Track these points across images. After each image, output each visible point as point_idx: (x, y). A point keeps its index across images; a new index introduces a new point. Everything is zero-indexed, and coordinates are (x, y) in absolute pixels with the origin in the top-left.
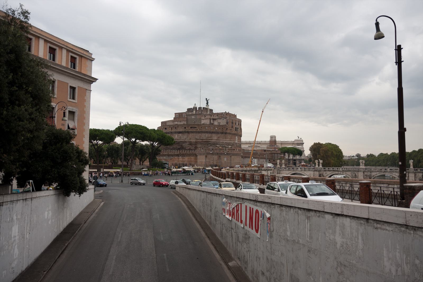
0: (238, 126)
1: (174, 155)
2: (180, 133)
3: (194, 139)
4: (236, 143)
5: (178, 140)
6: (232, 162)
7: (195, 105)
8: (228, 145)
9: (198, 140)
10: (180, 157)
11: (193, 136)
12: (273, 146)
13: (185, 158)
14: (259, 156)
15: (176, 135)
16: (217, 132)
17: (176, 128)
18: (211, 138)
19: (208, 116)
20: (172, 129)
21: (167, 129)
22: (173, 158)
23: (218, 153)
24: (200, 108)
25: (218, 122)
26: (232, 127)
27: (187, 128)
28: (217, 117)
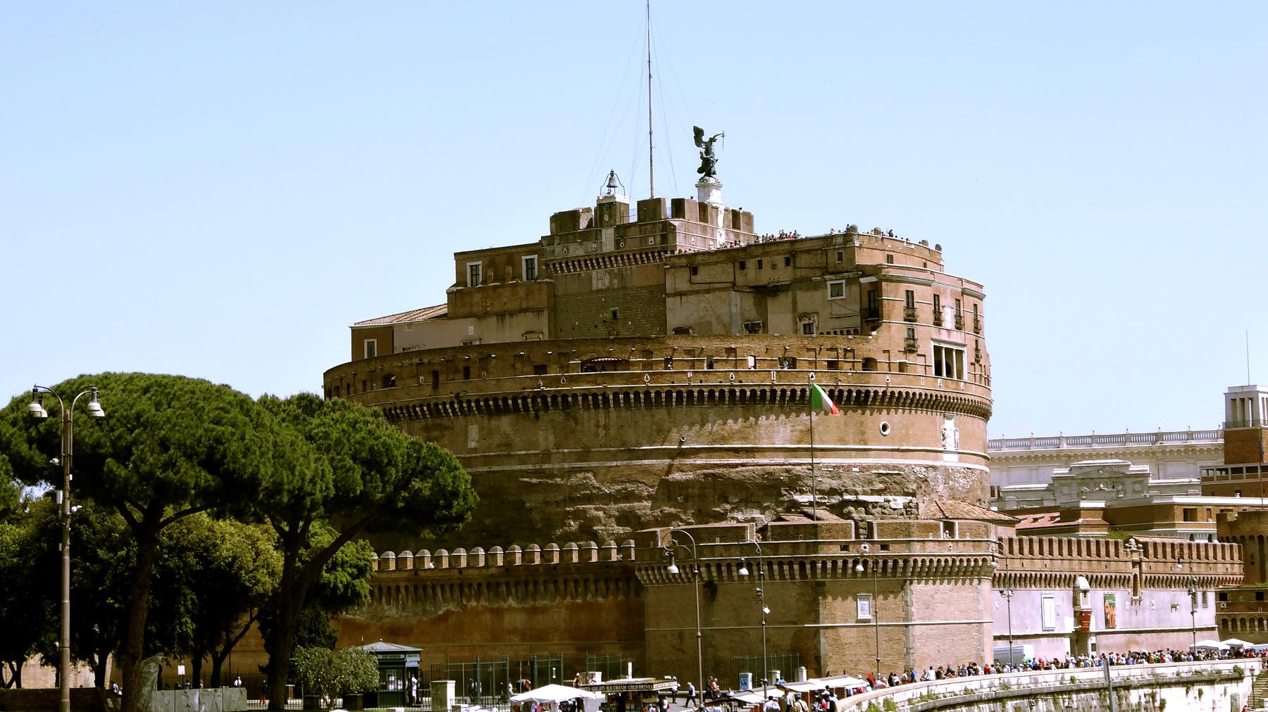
0: (957, 337)
4: (948, 474)
5: (485, 465)
8: (879, 492)
10: (512, 602)
11: (606, 427)
12: (1249, 470)
14: (1139, 563)
15: (474, 431)
18: (745, 439)
19: (718, 268)
20: (442, 378)
22: (452, 607)
23: (802, 565)
24: (649, 208)
25: (794, 309)
28: (784, 275)
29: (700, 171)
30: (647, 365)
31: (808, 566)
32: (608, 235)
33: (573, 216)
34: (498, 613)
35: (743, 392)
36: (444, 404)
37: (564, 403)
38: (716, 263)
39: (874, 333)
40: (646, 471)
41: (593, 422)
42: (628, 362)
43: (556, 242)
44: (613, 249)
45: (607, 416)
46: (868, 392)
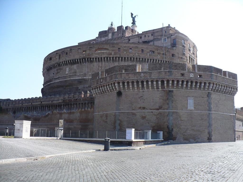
0: (193, 55)
1: (52, 106)
2: (74, 62)
5: (70, 78)
6: (213, 116)
7: (112, 25)
10: (65, 111)
11: (101, 67)
13: (73, 113)
15: (67, 69)
16: (153, 60)
17: (67, 53)
20: (61, 56)
22: (49, 112)
23: (163, 82)
24: (120, 28)
28: (151, 38)
29: (132, 23)
30: (113, 50)
31: (165, 82)
34: (61, 114)
35: (140, 59)
38: (135, 38)
44: (111, 38)
45: (102, 64)
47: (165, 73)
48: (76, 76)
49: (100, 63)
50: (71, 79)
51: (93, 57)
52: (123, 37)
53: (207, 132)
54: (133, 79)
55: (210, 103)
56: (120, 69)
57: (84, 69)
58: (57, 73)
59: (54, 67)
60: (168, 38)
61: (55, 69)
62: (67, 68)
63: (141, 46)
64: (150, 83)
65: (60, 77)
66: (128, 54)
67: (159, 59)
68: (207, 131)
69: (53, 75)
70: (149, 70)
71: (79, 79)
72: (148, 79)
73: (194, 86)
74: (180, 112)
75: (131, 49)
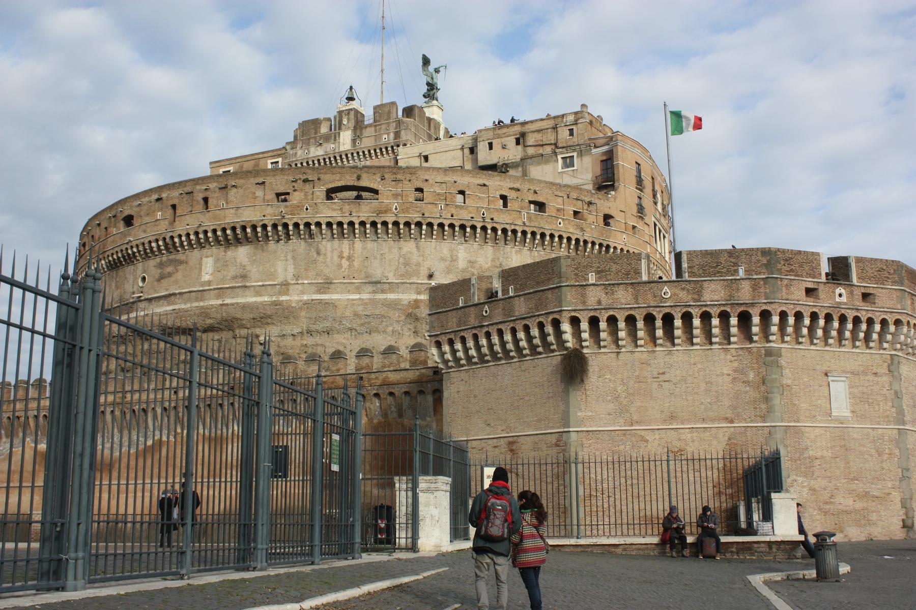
3: (358, 290)
5: (218, 297)
9: (391, 296)
11: (349, 258)
17: (206, 200)
20: (179, 212)
21: (136, 222)
23: (744, 318)
26: (641, 209)
27: (295, 198)
28: (514, 153)
30: (396, 196)
31: (756, 320)
32: (346, 139)
33: (316, 123)
35: (494, 230)
36: (180, 236)
37: (308, 230)
39: (613, 193)
40: (393, 305)
41: (336, 254)
42: (376, 192)
43: (299, 146)
45: (352, 247)
46: (608, 247)
47: (755, 288)
48: (247, 292)
49: (346, 242)
50: (227, 305)
51: (316, 220)
52: (398, 146)
53: (898, 501)
54: (631, 308)
55: (897, 395)
56: (576, 269)
57: (280, 263)
58: (161, 278)
59: (148, 254)
60: (581, 154)
61: (152, 263)
62: (207, 257)
63: (498, 183)
64: (697, 322)
65: (174, 294)
66: (453, 211)
67: (561, 233)
68: (896, 496)
69: (141, 284)
70: (692, 274)
71: (261, 303)
72: (690, 310)
73: (848, 334)
74: (807, 429)
75: (462, 192)
